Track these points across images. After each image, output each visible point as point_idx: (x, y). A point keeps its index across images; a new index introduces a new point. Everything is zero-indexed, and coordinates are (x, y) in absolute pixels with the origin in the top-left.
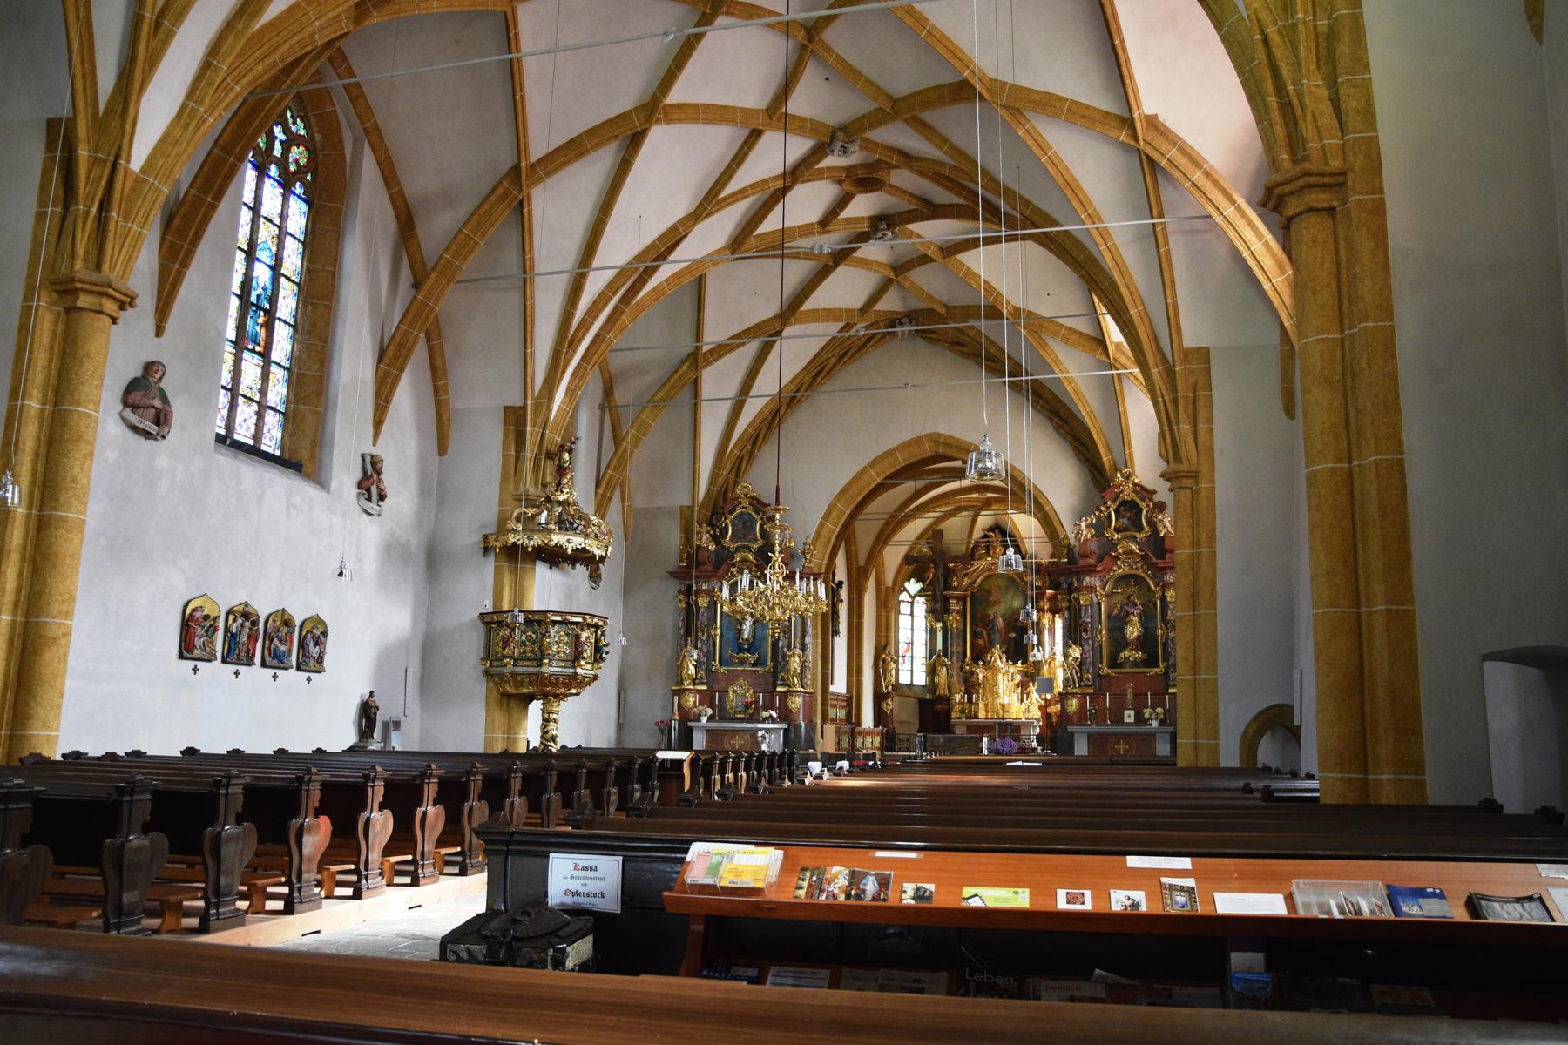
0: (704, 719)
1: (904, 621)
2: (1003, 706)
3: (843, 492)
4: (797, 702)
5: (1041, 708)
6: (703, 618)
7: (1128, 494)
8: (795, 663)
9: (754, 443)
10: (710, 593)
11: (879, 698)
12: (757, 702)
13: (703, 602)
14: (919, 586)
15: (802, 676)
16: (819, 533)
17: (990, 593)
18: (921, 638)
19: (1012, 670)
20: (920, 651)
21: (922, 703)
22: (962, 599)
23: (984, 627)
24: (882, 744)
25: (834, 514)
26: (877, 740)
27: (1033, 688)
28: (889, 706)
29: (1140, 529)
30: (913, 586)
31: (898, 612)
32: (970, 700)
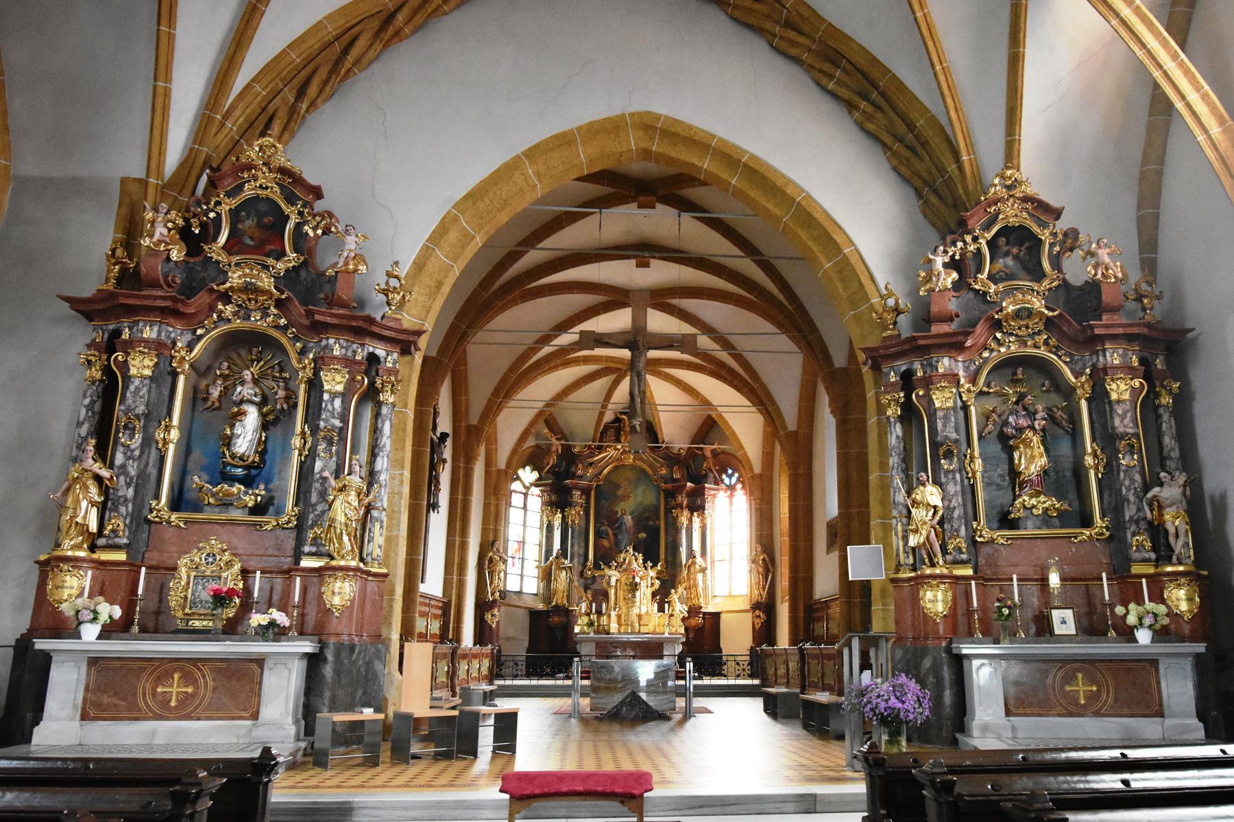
0: (90, 632)
1: (515, 515)
2: (640, 617)
3: (473, 197)
4: (340, 592)
5: (683, 620)
6: (135, 399)
7: (1012, 214)
8: (344, 509)
9: (301, 93)
10: (161, 348)
11: (482, 607)
12: (248, 591)
13: (141, 366)
14: (535, 475)
15: (361, 541)
16: (419, 265)
17: (618, 486)
18: (535, 537)
19: (652, 573)
20: (533, 553)
21: (534, 614)
22: (586, 492)
23: (610, 525)
24: (491, 670)
25: (453, 236)
26: (486, 663)
27: (674, 597)
28: (494, 618)
29: (1039, 275)
30: (528, 475)
31: (509, 504)
32: (599, 613)
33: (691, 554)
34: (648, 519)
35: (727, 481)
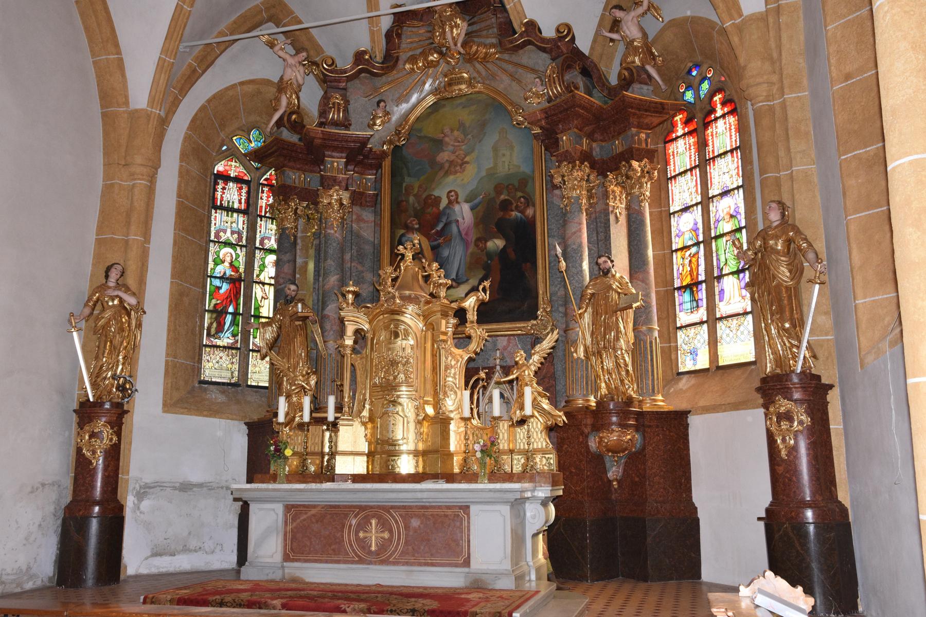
17: (438, 144)
33: (602, 273)
34: (506, 206)
35: (689, 96)
